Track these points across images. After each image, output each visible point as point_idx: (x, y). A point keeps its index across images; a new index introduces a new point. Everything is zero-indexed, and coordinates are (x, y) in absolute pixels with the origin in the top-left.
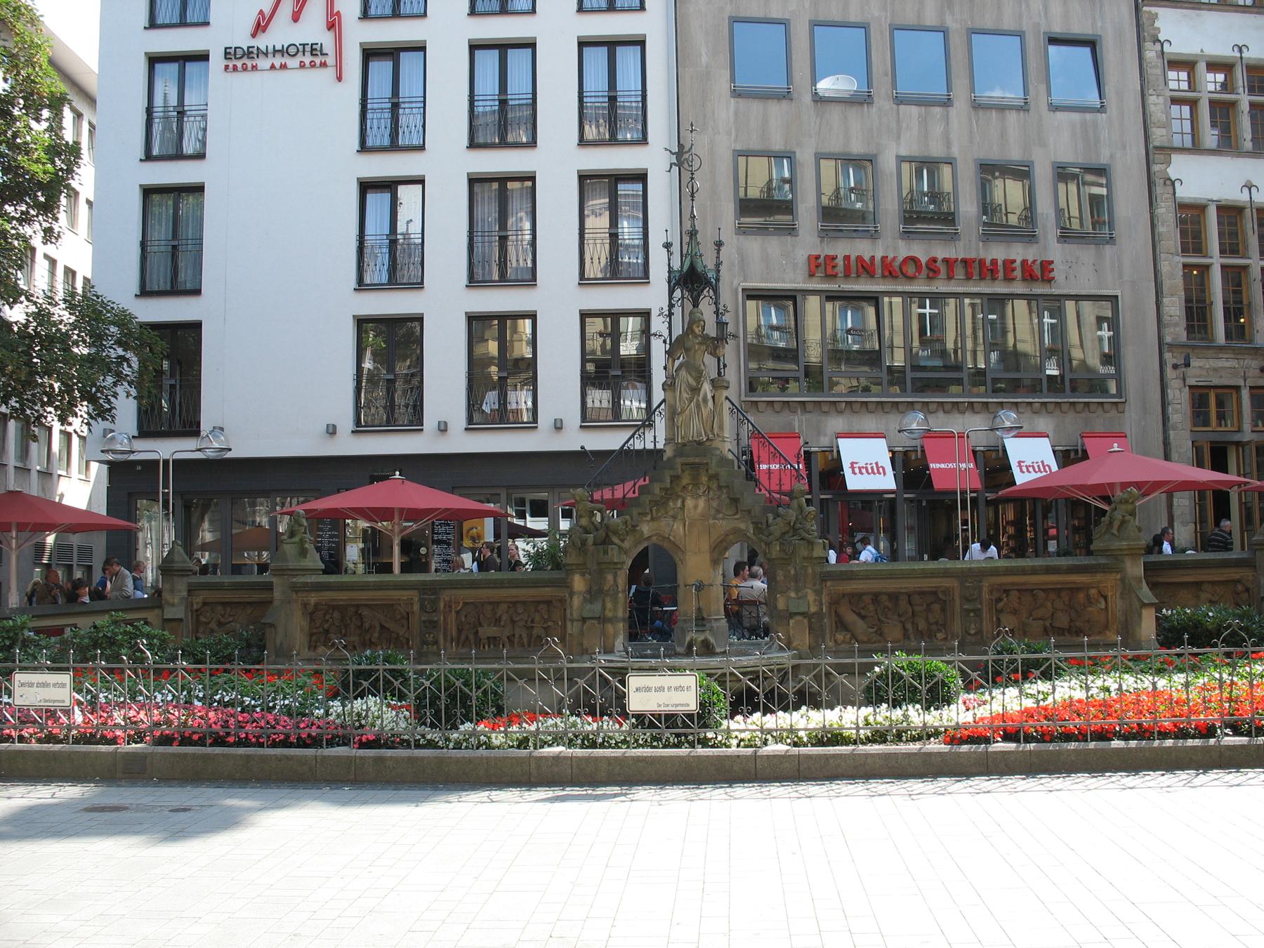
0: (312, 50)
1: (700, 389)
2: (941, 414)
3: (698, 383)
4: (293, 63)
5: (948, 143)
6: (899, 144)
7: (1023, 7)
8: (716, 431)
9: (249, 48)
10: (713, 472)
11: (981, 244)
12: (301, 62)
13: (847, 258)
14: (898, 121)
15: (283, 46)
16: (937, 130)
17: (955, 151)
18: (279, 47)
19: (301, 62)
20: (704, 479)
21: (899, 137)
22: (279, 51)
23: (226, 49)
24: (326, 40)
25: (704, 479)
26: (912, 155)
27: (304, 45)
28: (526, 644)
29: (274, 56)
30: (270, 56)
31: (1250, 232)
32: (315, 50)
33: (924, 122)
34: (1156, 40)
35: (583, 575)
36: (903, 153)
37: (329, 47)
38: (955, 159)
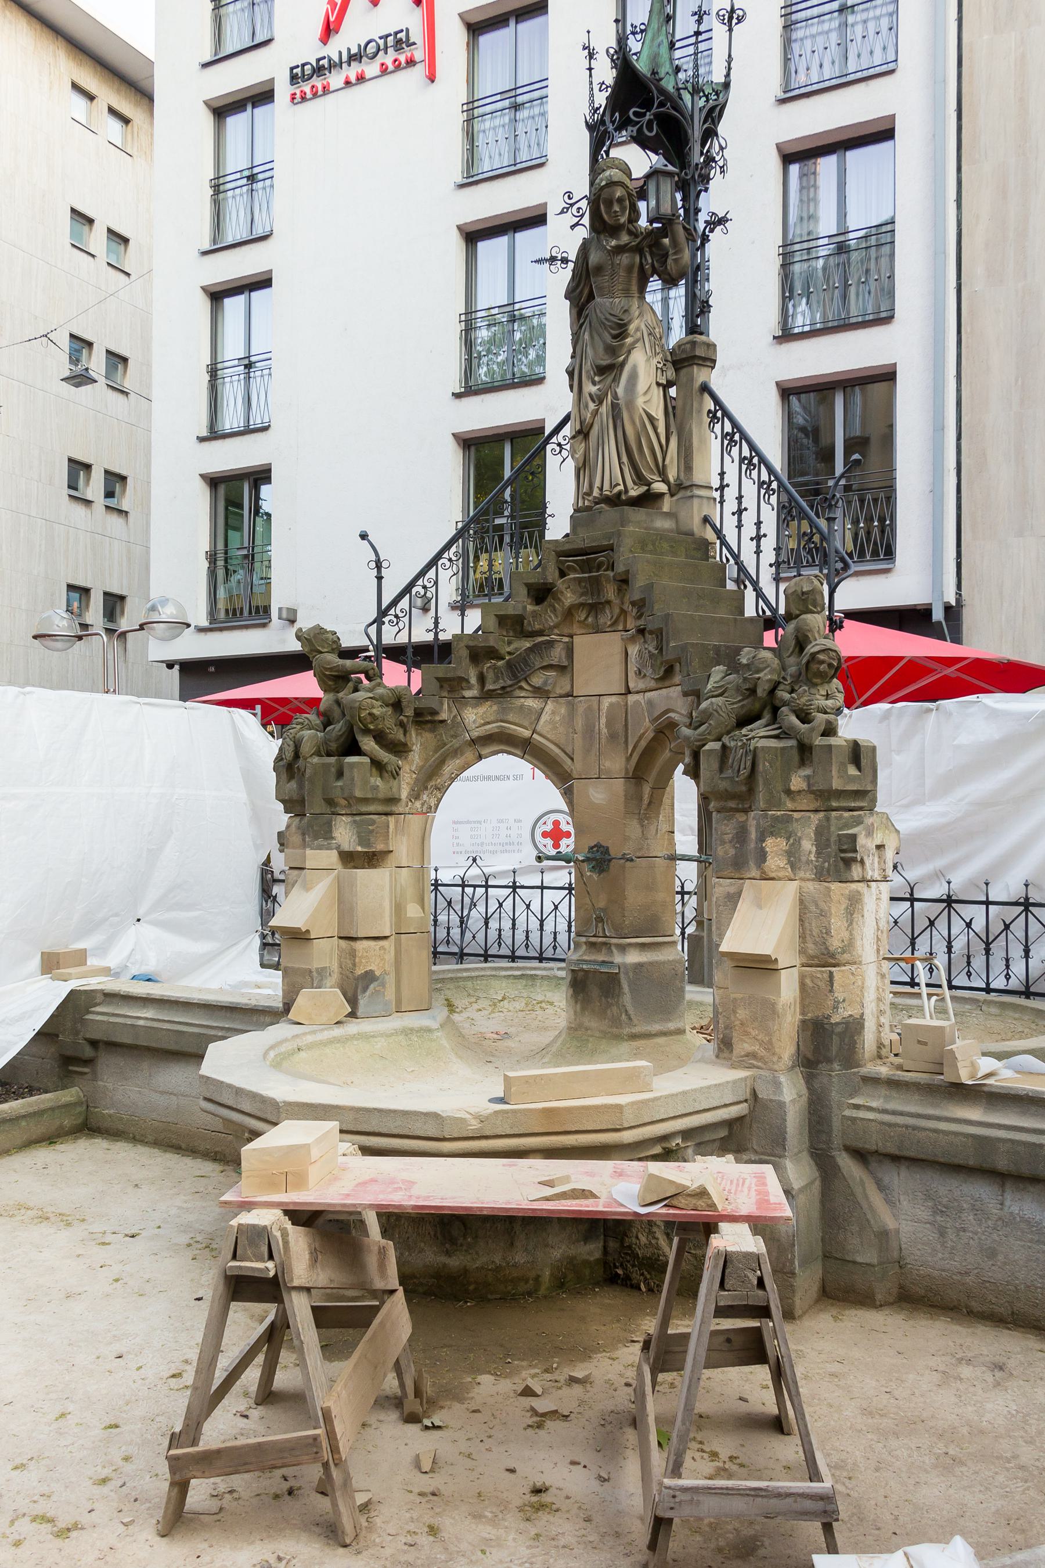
0: (399, 42)
1: (623, 365)
3: (612, 351)
4: (371, 69)
8: (672, 475)
9: (318, 60)
12: (382, 64)
15: (359, 46)
18: (354, 50)
19: (382, 64)
20: (610, 592)
22: (355, 55)
23: (292, 69)
24: (413, 21)
25: (610, 592)
27: (385, 37)
29: (349, 65)
30: (344, 66)
32: (401, 42)
37: (417, 35)
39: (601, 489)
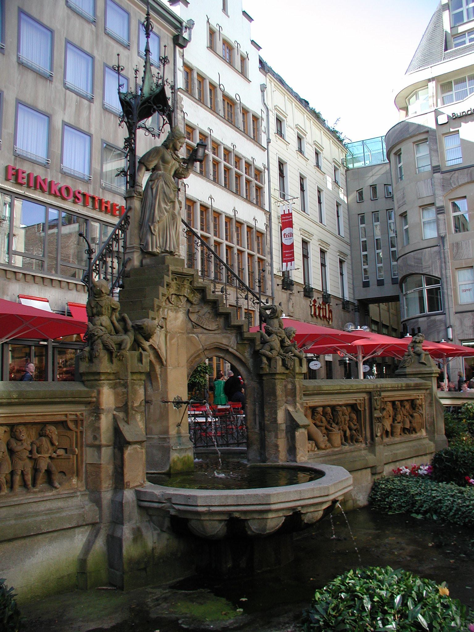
2: (74, 292)
5: (90, 124)
6: (65, 114)
7: (130, 64)
10: (200, 285)
11: (101, 190)
13: (29, 175)
14: (65, 100)
16: (85, 114)
17: (93, 131)
21: (65, 109)
26: (71, 123)
28: (29, 482)
31: (211, 221)
33: (79, 107)
34: (182, 111)
35: (114, 387)
36: (66, 120)
38: (92, 135)
39: (170, 248)
